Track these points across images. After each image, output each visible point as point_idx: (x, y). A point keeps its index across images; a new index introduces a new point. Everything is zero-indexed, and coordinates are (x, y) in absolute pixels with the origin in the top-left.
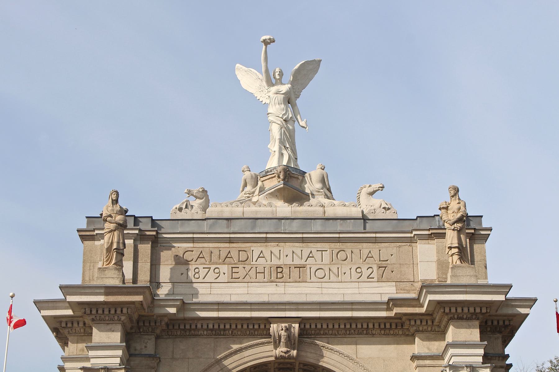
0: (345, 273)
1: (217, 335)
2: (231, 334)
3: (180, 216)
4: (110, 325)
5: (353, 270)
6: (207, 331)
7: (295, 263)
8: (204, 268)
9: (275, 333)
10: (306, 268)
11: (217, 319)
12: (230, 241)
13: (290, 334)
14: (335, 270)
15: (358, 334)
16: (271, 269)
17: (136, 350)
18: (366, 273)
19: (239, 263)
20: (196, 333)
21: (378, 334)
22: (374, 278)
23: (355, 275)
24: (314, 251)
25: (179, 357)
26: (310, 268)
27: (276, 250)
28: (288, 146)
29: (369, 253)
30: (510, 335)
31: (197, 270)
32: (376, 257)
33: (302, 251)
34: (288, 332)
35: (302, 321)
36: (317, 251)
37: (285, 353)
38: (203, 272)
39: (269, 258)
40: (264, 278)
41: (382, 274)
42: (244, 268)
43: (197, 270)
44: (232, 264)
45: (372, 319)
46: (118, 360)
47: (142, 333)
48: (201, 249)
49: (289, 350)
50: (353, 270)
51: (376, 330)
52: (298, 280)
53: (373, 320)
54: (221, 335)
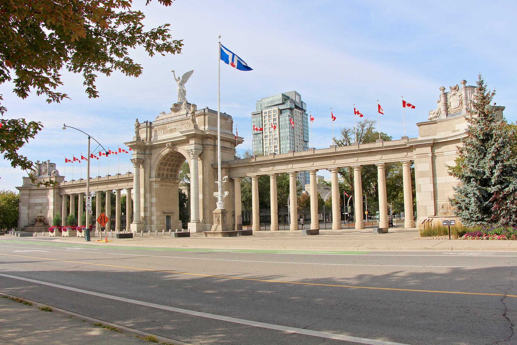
3: (157, 120)
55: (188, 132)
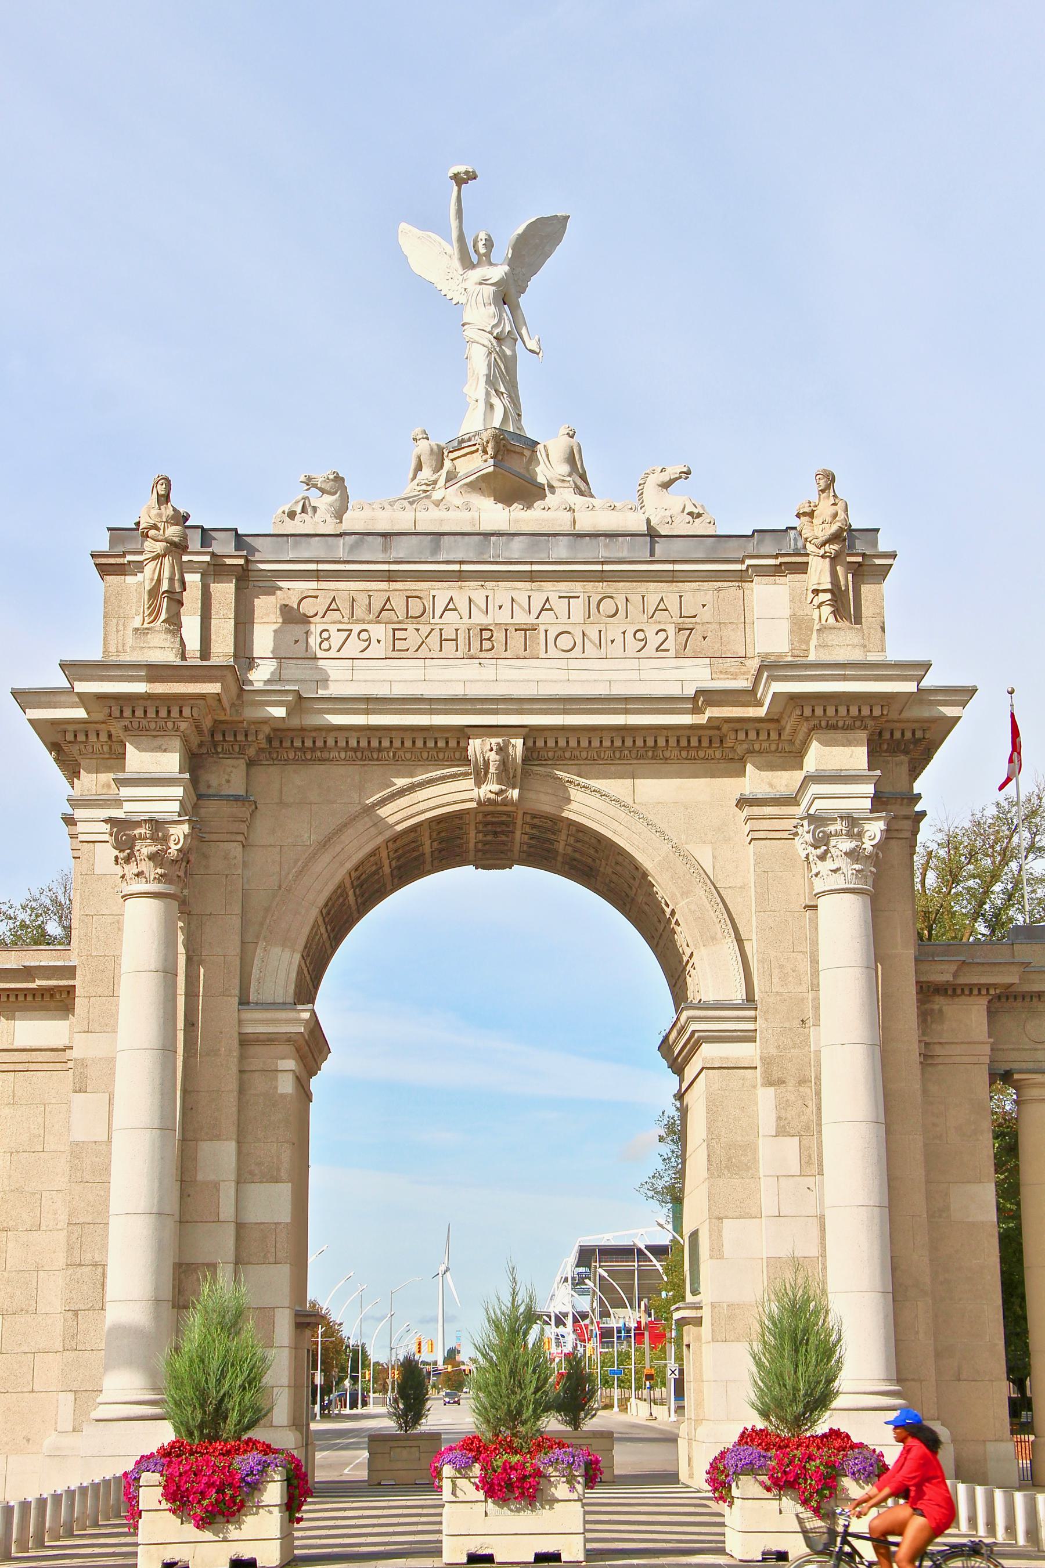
0: (612, 641)
1: (365, 760)
2: (392, 757)
4: (159, 738)
5: (629, 635)
6: (346, 752)
7: (515, 621)
8: (339, 630)
9: (478, 756)
10: (539, 633)
11: (366, 730)
12: (389, 577)
13: (506, 758)
14: (593, 633)
15: (636, 758)
16: (469, 633)
17: (209, 787)
18: (654, 641)
19: (407, 620)
20: (325, 755)
21: (676, 758)
22: (668, 650)
23: (633, 645)
24: (554, 598)
25: (292, 801)
26: (546, 631)
27: (479, 597)
28: (502, 389)
29: (660, 602)
30: (926, 757)
31: (325, 635)
32: (674, 610)
33: (529, 597)
34: (503, 754)
35: (530, 733)
36: (560, 597)
37: (496, 794)
38: (337, 638)
39: (465, 612)
40: (457, 650)
41: (684, 643)
42: (418, 630)
43: (325, 635)
44: (393, 623)
45: (665, 729)
46: (176, 806)
47: (221, 756)
48: (333, 594)
49: (504, 788)
50: (629, 635)
51: (671, 751)
52: (522, 653)
53: (666, 731)
54: (372, 759)
55: (845, 678)
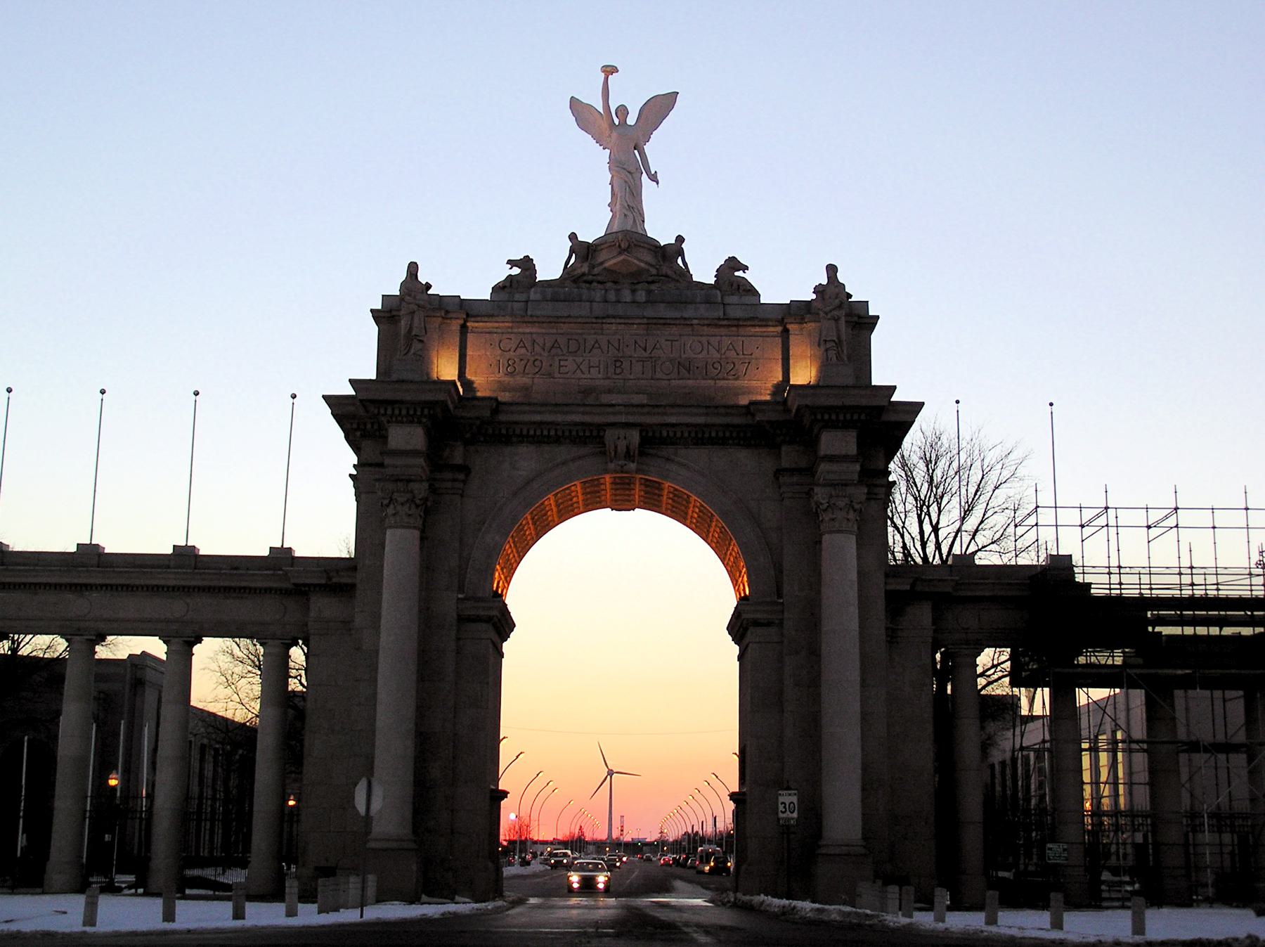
35: (642, 428)
